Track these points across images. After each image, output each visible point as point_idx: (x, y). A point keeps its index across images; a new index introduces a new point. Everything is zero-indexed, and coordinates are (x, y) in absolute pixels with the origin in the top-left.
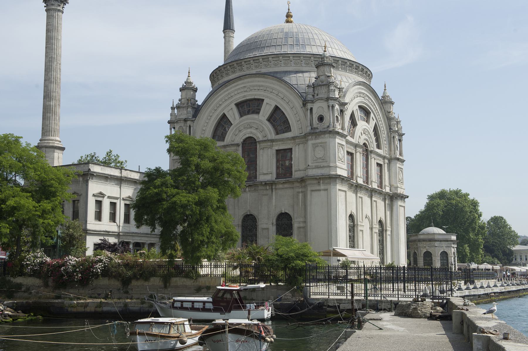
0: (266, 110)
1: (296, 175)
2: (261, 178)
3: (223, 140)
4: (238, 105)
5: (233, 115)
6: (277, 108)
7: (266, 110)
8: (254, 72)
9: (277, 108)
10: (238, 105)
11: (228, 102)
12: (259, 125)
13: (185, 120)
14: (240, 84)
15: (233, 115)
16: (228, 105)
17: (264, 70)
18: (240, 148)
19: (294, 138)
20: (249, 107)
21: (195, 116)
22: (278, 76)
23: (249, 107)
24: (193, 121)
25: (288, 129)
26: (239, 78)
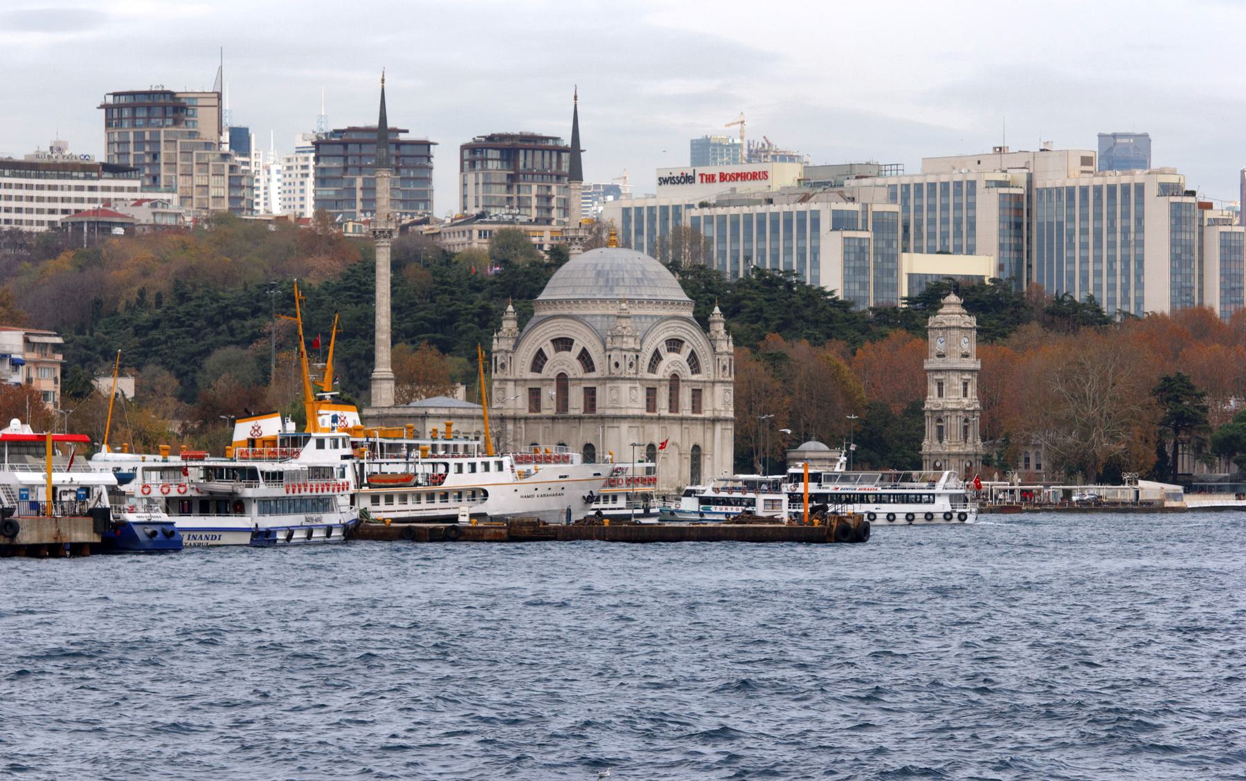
0: (576, 350)
1: (599, 412)
2: (571, 412)
3: (540, 372)
4: (553, 341)
5: (549, 350)
6: (584, 350)
7: (576, 350)
8: (566, 312)
9: (584, 350)
10: (553, 341)
12: (569, 362)
13: (507, 352)
14: (554, 323)
15: (549, 350)
19: (597, 379)
20: (563, 344)
21: (515, 347)
22: (587, 319)
23: (563, 344)
25: (593, 370)
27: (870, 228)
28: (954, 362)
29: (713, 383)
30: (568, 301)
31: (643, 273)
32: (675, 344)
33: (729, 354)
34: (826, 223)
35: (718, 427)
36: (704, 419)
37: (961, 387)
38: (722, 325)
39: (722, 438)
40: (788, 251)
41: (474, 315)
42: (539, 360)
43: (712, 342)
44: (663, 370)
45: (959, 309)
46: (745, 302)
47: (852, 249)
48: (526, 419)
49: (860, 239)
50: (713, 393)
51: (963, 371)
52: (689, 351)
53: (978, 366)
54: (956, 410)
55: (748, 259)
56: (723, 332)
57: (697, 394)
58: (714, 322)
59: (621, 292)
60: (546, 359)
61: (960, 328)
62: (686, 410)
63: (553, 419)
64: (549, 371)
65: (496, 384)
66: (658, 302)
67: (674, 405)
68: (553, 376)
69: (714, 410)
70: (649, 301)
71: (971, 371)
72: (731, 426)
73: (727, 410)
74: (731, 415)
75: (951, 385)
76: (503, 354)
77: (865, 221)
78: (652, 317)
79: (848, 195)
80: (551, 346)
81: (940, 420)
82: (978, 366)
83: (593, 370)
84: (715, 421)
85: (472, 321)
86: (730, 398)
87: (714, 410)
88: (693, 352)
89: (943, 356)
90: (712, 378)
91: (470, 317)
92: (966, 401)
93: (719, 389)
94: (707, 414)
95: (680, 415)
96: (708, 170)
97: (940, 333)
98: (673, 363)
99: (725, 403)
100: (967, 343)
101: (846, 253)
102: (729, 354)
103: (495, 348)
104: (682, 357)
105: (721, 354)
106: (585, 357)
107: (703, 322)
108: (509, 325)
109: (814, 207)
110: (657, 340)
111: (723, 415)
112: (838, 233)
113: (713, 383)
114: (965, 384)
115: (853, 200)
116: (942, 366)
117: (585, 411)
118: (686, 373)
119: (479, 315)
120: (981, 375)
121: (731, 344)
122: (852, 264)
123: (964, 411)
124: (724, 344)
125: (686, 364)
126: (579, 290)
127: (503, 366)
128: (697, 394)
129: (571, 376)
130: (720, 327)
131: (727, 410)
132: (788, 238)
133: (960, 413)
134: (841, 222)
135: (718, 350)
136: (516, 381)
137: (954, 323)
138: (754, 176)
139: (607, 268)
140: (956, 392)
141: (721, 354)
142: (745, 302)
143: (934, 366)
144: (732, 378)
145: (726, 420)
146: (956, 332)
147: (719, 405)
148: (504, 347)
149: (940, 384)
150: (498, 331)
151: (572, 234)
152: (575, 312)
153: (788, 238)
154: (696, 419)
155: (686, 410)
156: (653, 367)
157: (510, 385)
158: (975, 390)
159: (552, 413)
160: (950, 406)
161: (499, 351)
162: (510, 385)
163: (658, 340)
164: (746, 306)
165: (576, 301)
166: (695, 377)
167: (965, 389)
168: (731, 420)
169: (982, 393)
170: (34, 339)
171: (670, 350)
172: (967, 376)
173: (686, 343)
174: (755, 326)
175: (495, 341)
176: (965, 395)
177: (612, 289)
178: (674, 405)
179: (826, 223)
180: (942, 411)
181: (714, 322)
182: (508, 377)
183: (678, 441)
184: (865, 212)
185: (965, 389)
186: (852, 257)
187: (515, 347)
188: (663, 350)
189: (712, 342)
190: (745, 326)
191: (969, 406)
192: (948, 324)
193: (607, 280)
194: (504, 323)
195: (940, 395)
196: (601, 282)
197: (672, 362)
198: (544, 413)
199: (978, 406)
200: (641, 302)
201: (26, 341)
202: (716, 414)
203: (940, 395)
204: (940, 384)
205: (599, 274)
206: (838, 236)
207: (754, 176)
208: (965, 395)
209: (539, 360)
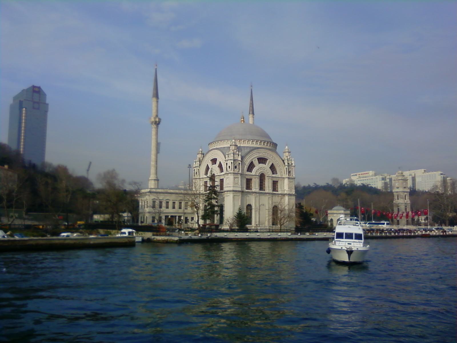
0: (218, 163)
4: (211, 160)
7: (218, 163)
11: (208, 160)
16: (254, 158)
17: (218, 147)
21: (200, 165)
24: (199, 167)
32: (262, 160)
52: (270, 164)
67: (262, 186)
80: (210, 161)
81: (398, 206)
92: (406, 201)
96: (359, 173)
110: (253, 157)
118: (268, 172)
138: (367, 173)
140: (403, 198)
163: (253, 157)
166: (274, 175)
168: (294, 195)
171: (259, 163)
176: (405, 199)
178: (262, 186)
180: (399, 204)
187: (200, 165)
188: (256, 162)
197: (258, 168)
199: (409, 202)
203: (398, 199)
207: (367, 173)
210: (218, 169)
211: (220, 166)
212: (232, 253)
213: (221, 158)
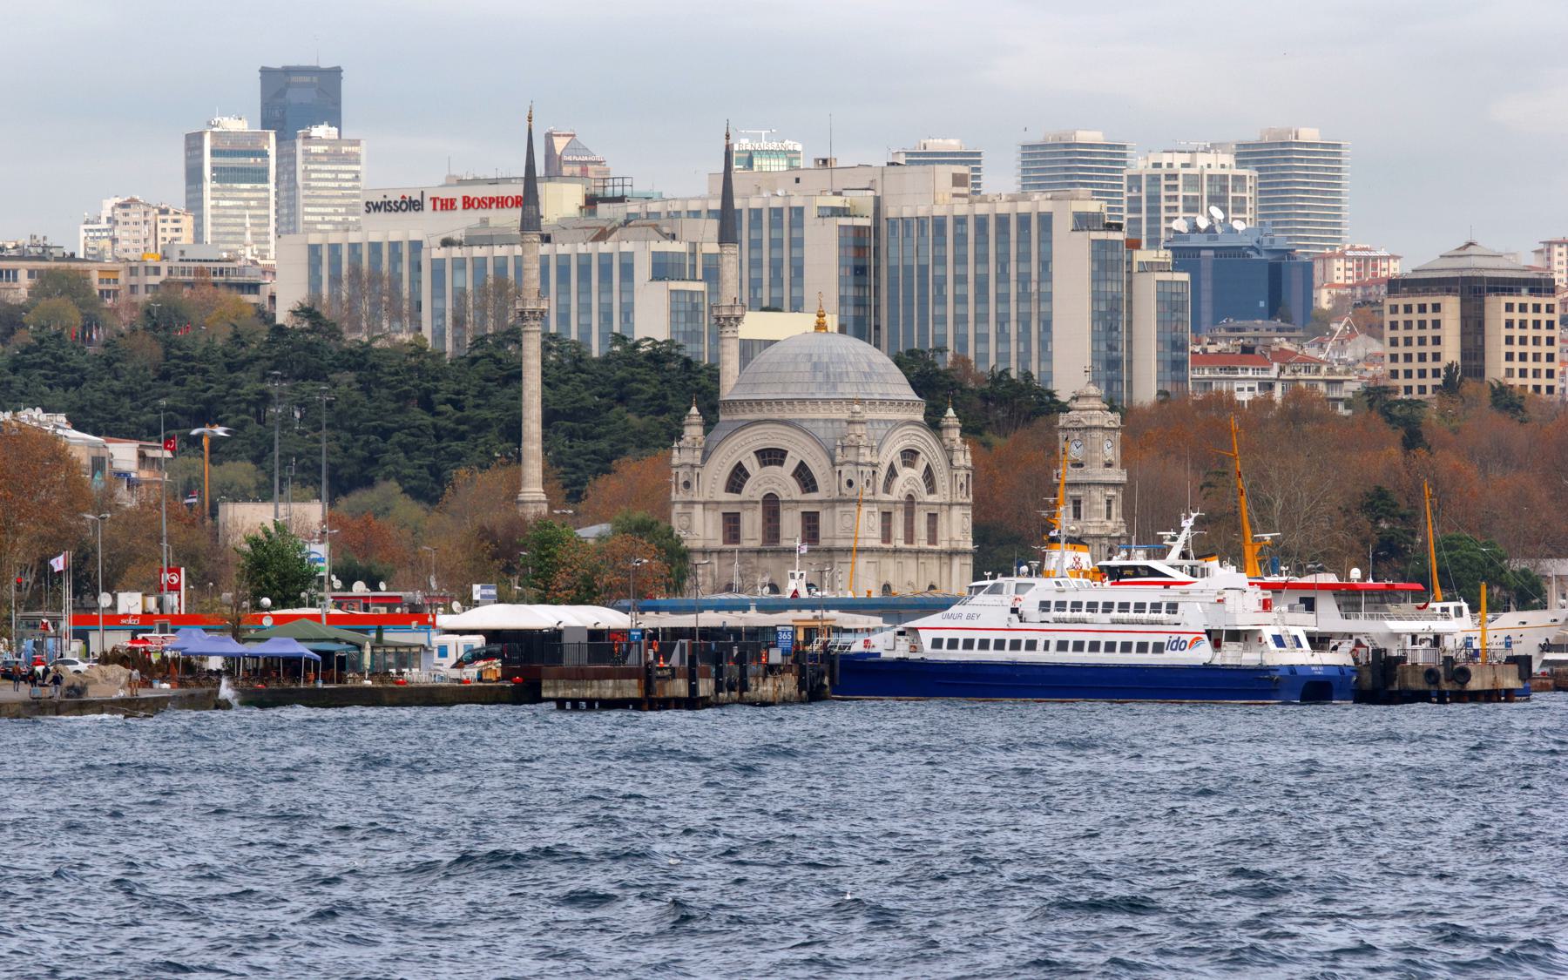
0: (791, 464)
3: (739, 492)
4: (756, 453)
5: (752, 465)
6: (802, 463)
7: (791, 464)
8: (776, 416)
9: (802, 463)
10: (756, 453)
12: (781, 480)
13: (693, 466)
15: (752, 465)
18: (760, 506)
19: (821, 502)
20: (772, 456)
21: (705, 459)
22: (805, 425)
23: (772, 456)
25: (815, 489)
26: (758, 422)
27: (699, 275)
28: (1097, 473)
29: (950, 505)
30: (779, 402)
31: (870, 364)
33: (966, 468)
34: (643, 270)
35: (957, 561)
36: (941, 552)
37: (1104, 507)
38: (958, 431)
39: (961, 575)
40: (585, 309)
41: (249, 403)
42: (738, 478)
43: (949, 452)
44: (899, 490)
45: (1098, 404)
46: (635, 385)
47: (682, 307)
48: (720, 552)
49: (692, 293)
50: (949, 518)
51: (1106, 485)
53: (1124, 479)
54: (1100, 537)
55: (459, 322)
56: (959, 440)
57: (933, 518)
58: (948, 427)
59: (848, 391)
60: (747, 475)
61: (1103, 428)
62: (922, 543)
63: (759, 552)
64: (754, 489)
65: (678, 508)
66: (892, 402)
67: (910, 536)
68: (759, 498)
69: (951, 540)
70: (882, 402)
71: (1115, 485)
72: (969, 560)
73: (965, 540)
74: (969, 546)
75: (1091, 504)
76: (688, 469)
77: (694, 267)
78: (886, 422)
79: (666, 230)
82: (1124, 479)
83: (815, 489)
84: (952, 553)
85: (246, 411)
86: (968, 524)
87: (951, 540)
88: (928, 467)
89: (1081, 465)
90: (948, 500)
91: (243, 406)
92: (1110, 524)
93: (957, 512)
94: (943, 545)
95: (915, 546)
97: (1077, 435)
98: (909, 481)
99: (964, 531)
100: (1110, 449)
101: (674, 312)
102: (966, 468)
103: (675, 461)
104: (917, 473)
105: (958, 468)
106: (804, 476)
107: (934, 424)
108: (693, 431)
109: (626, 247)
111: (961, 546)
112: (663, 284)
113: (950, 505)
114: (1109, 502)
115: (674, 237)
116: (1079, 478)
117: (725, 542)
119: (255, 403)
120: (1126, 489)
121: (968, 456)
122: (682, 328)
123: (1110, 538)
124: (961, 455)
125: (921, 481)
126: (792, 388)
127: (687, 485)
128: (933, 518)
129: (783, 496)
130: (955, 434)
131: (965, 540)
132: (585, 289)
133: (1106, 541)
134: (663, 269)
135: (956, 464)
136: (704, 503)
137: (1095, 422)
139: (825, 359)
141: (958, 468)
142: (635, 385)
143: (1069, 479)
144: (970, 500)
145: (964, 553)
146: (1098, 434)
147: (957, 535)
148: (690, 461)
149: (1077, 503)
150: (680, 439)
151: (725, 313)
152: (788, 416)
153: (585, 289)
154: (932, 552)
155: (922, 543)
156: (887, 488)
157: (698, 509)
158: (1120, 511)
159: (757, 544)
160: (1092, 532)
161: (681, 466)
162: (698, 509)
164: (639, 391)
165: (790, 401)
166: (931, 498)
167: (1109, 509)
169: (1127, 514)
170: (150, 453)
171: (905, 464)
172: (1111, 492)
173: (922, 455)
174: (661, 419)
175: (676, 452)
176: (1109, 517)
177: (834, 386)
178: (910, 536)
179: (643, 270)
181: (948, 427)
182: (696, 498)
183: (914, 580)
184: (693, 254)
185: (1109, 509)
186: (682, 318)
187: (705, 459)
188: (898, 464)
189: (949, 452)
190: (646, 419)
191: (1114, 531)
192: (1087, 423)
193: (828, 376)
194: (687, 430)
195: (1077, 515)
196: (820, 377)
198: (746, 544)
200: (872, 402)
201: (142, 456)
202: (954, 545)
203: (1077, 515)
204: (1077, 503)
205: (815, 366)
206: (662, 290)
208: (1109, 517)
209: (738, 478)
210: (793, 484)
211: (804, 476)
212: (32, 787)
213: (799, 450)
